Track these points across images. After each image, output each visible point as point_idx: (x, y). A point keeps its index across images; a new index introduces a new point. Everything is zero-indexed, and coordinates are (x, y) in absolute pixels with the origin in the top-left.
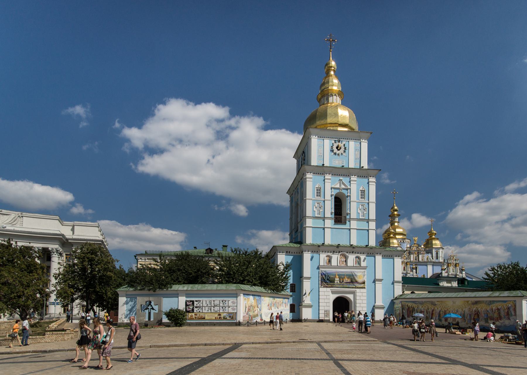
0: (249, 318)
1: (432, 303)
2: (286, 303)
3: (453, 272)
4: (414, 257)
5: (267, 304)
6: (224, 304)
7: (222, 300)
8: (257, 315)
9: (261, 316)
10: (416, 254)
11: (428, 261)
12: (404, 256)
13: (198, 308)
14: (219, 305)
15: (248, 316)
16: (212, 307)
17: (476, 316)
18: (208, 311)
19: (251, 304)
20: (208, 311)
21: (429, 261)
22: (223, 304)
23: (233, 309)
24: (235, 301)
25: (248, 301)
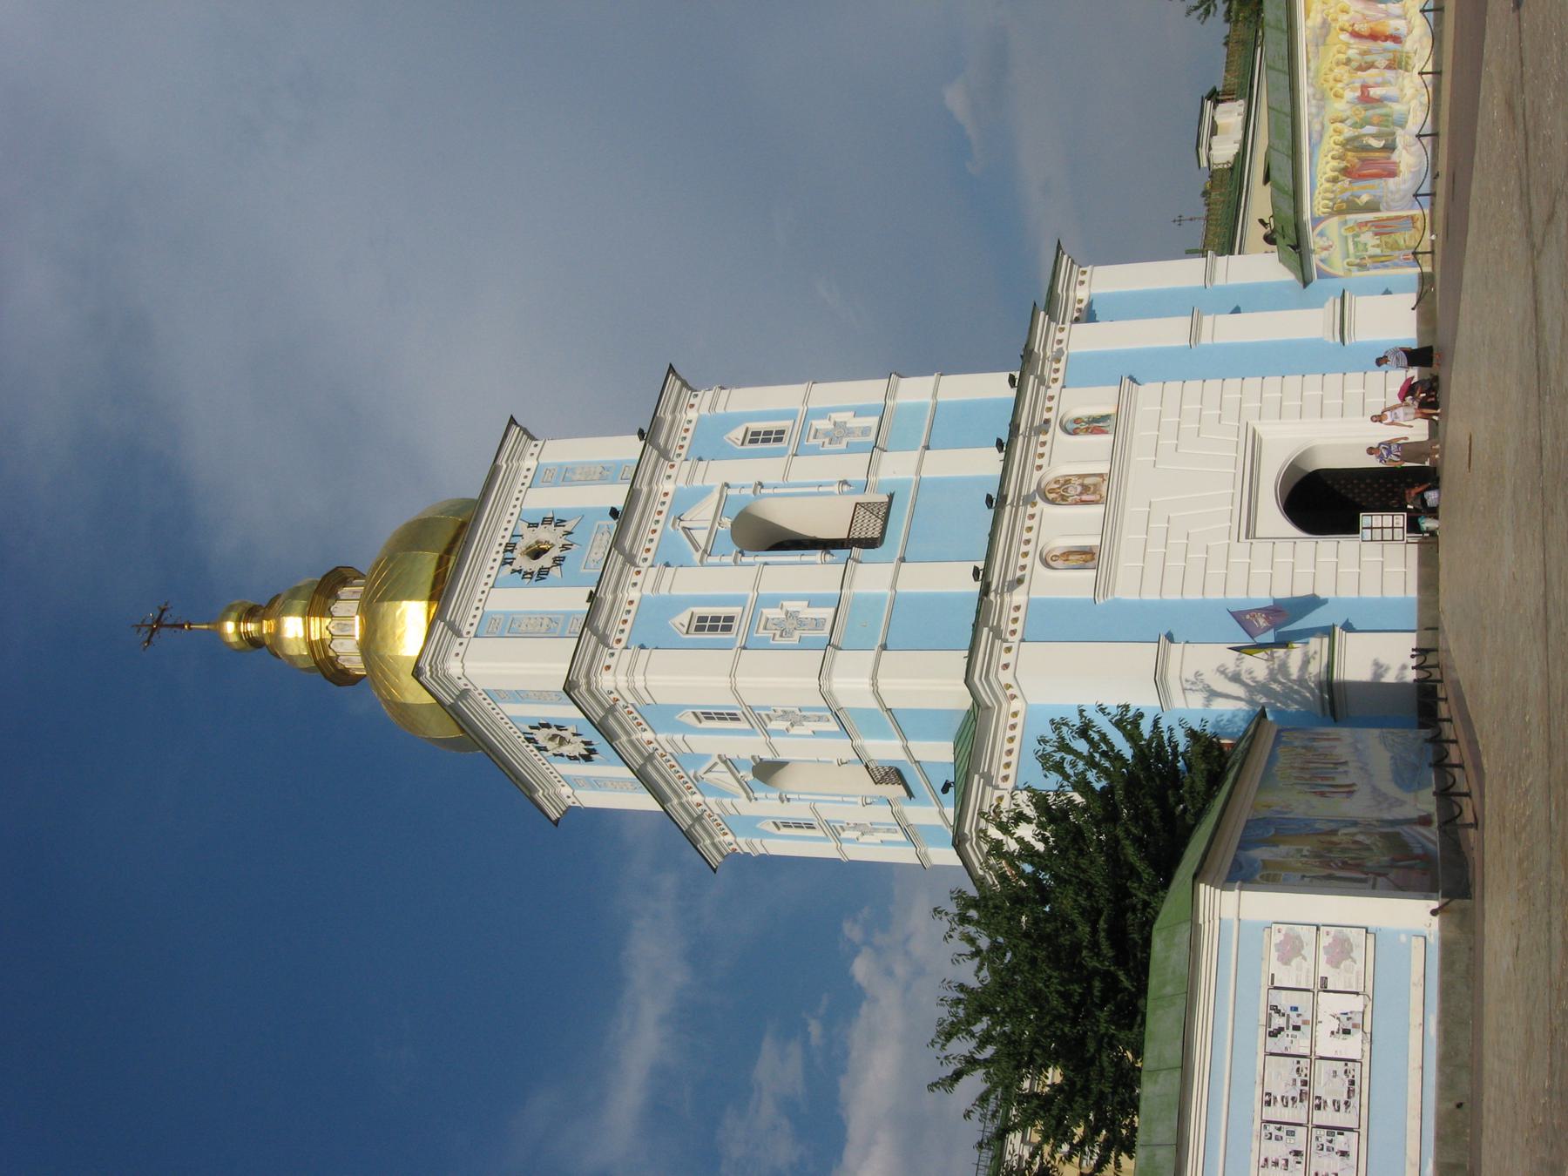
0: (1411, 867)
1: (1317, 46)
6: (1295, 1020)
7: (1262, 1031)
14: (1302, 1060)
16: (1326, 1117)
18: (1344, 1154)
20: (1344, 1154)
22: (1297, 1028)
23: (1340, 951)
24: (1277, 938)
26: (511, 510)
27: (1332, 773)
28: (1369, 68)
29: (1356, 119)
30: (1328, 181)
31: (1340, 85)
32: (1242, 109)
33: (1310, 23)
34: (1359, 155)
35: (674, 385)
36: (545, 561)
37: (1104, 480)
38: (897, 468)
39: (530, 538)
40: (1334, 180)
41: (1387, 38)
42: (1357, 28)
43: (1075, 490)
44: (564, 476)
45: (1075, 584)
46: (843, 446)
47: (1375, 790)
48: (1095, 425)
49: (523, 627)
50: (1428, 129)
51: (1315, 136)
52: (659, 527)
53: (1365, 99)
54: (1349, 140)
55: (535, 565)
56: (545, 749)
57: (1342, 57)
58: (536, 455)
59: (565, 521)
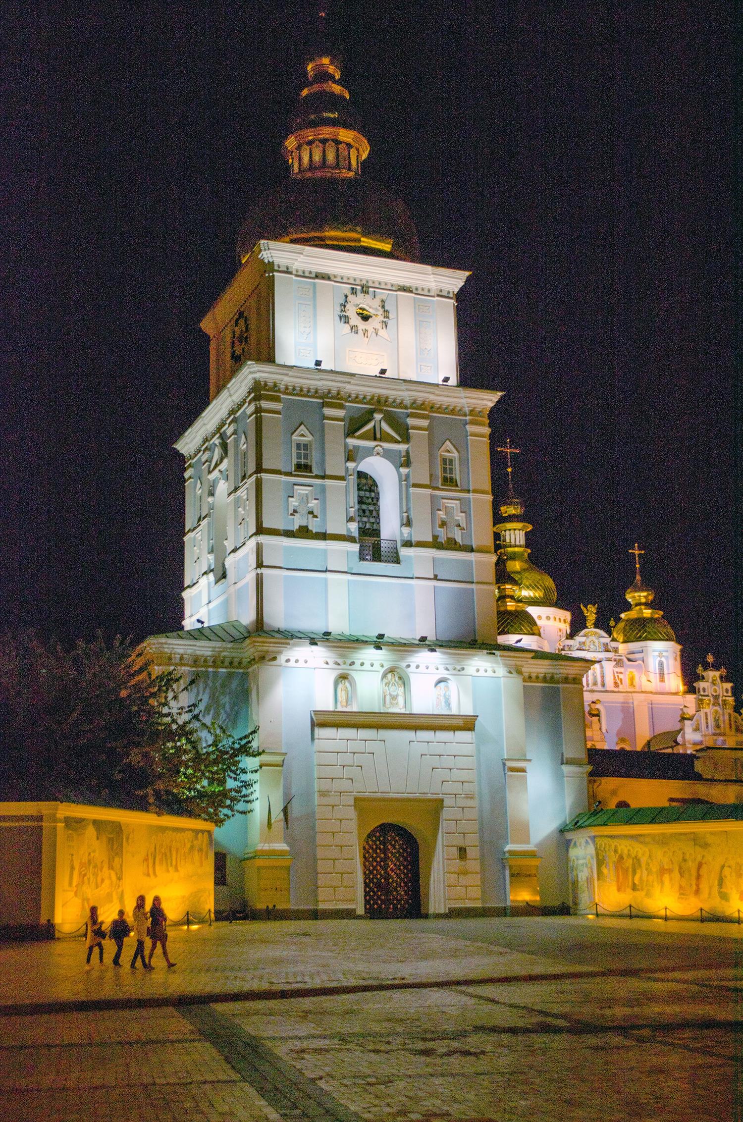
19: (90, 854)
21: (637, 690)
27: (167, 863)
28: (680, 873)
29: (651, 866)
30: (616, 847)
31: (671, 854)
34: (631, 867)
36: (355, 320)
37: (401, 709)
40: (616, 851)
41: (697, 885)
42: (704, 866)
51: (642, 839)
54: (639, 860)
55: (351, 312)
56: (236, 324)
57: (687, 857)
59: (386, 326)
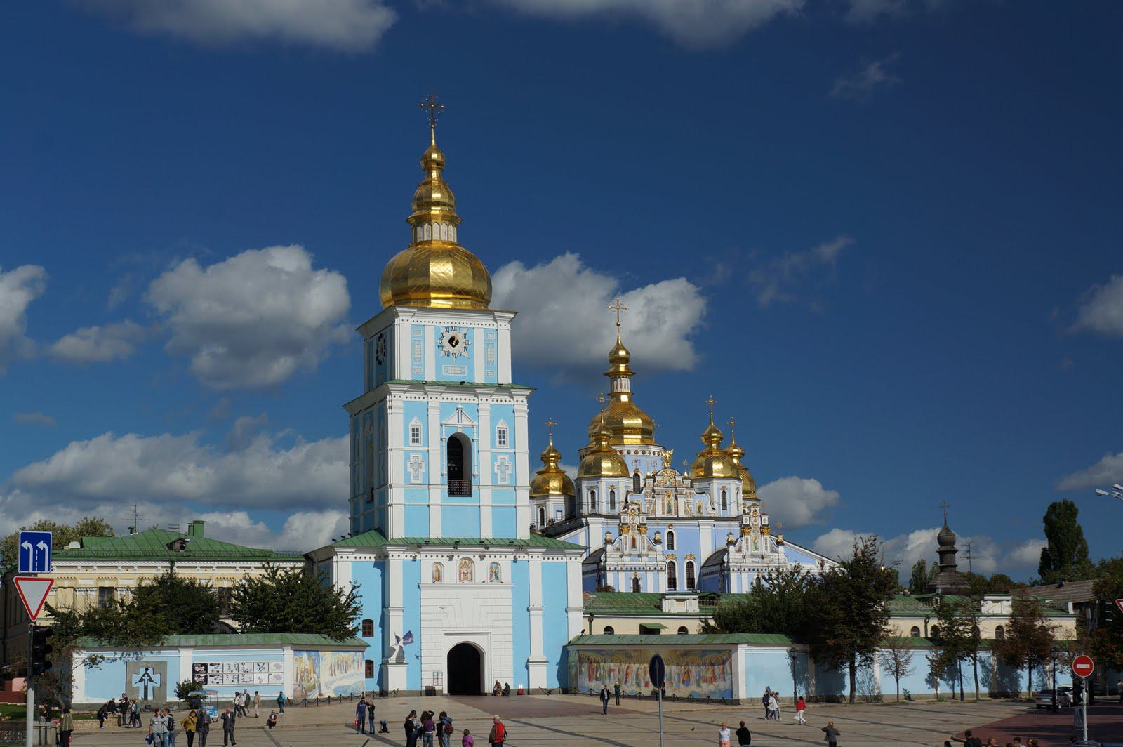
0: (302, 692)
2: (358, 662)
3: (756, 548)
4: (663, 504)
5: (329, 666)
7: (258, 661)
8: (313, 687)
9: (319, 688)
10: (669, 496)
11: (700, 515)
12: (633, 509)
13: (216, 677)
15: (300, 689)
17: (686, 675)
21: (705, 515)
23: (278, 678)
25: (301, 662)
26: (473, 322)
32: (691, 611)
33: (632, 652)
35: (527, 392)
36: (448, 346)
38: (484, 494)
39: (460, 337)
40: (589, 659)
43: (465, 570)
44: (492, 343)
45: (426, 577)
46: (496, 471)
47: (333, 682)
48: (494, 575)
49: (417, 346)
50: (593, 693)
52: (459, 401)
53: (611, 670)
58: (499, 327)
